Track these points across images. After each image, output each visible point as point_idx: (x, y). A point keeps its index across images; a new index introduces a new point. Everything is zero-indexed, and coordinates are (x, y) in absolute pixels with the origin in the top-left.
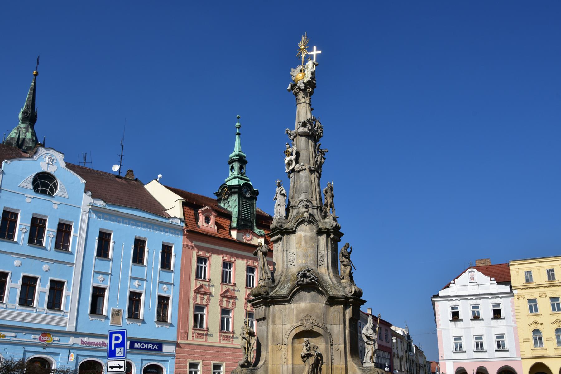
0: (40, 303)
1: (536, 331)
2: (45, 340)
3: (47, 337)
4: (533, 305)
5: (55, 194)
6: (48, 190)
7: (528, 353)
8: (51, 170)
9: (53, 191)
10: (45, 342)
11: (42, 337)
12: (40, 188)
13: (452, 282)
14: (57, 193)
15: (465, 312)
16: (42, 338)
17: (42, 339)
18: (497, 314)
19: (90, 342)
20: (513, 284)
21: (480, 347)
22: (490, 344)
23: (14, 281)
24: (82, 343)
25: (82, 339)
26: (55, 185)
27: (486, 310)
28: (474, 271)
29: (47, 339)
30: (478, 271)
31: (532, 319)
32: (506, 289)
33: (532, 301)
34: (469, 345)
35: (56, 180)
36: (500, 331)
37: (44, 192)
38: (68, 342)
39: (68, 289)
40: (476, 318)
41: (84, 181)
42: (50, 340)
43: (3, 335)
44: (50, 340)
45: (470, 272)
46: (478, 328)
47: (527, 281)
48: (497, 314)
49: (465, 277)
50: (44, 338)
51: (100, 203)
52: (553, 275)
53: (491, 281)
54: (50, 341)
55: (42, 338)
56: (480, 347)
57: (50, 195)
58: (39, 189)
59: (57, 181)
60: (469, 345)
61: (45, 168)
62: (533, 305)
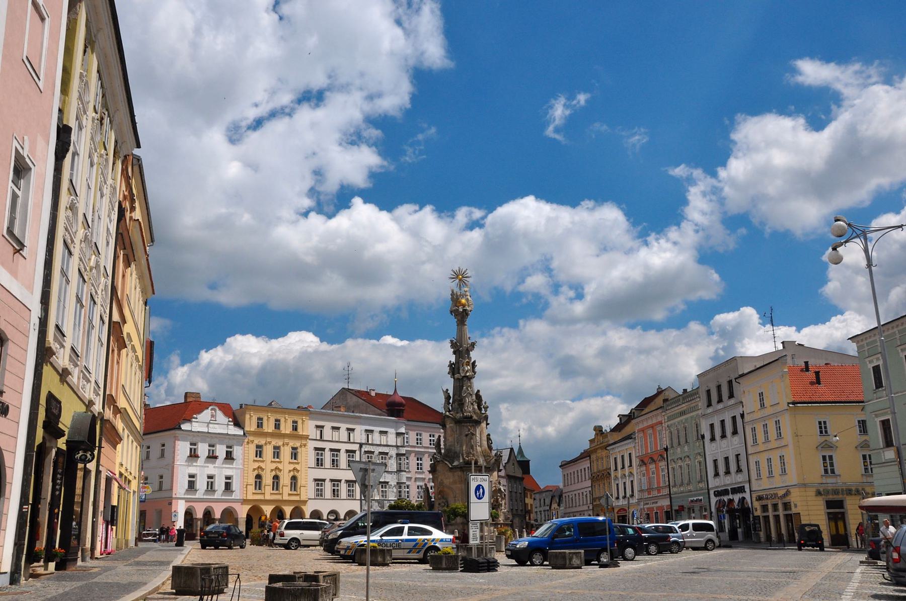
1: (258, 477)
4: (259, 451)
7: (250, 497)
13: (195, 416)
15: (203, 449)
18: (229, 456)
20: (247, 429)
21: (211, 487)
22: (220, 485)
27: (221, 451)
28: (214, 410)
30: (220, 409)
31: (256, 465)
32: (241, 433)
33: (259, 447)
34: (201, 484)
36: (229, 473)
40: (212, 457)
45: (212, 410)
46: (211, 469)
47: (258, 427)
48: (229, 456)
49: (206, 415)
52: (279, 425)
53: (229, 421)
56: (211, 487)
60: (201, 484)
62: (259, 451)
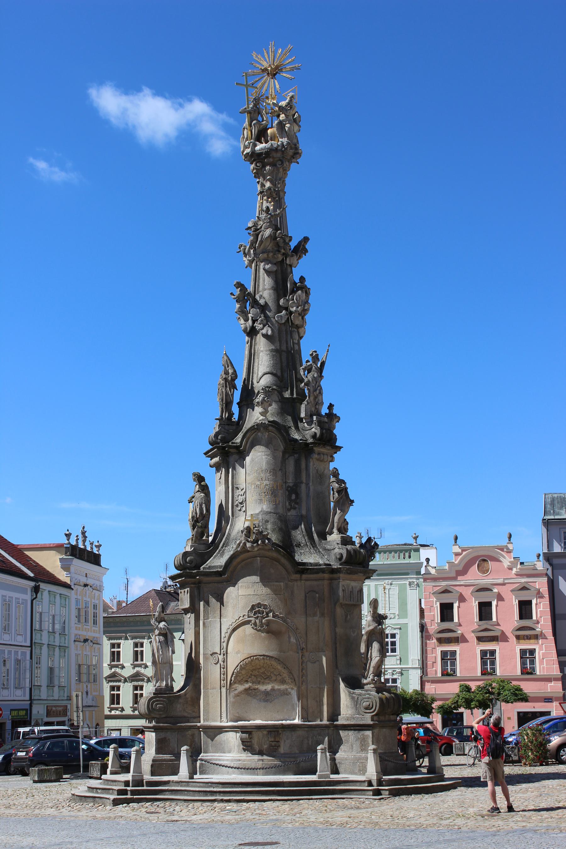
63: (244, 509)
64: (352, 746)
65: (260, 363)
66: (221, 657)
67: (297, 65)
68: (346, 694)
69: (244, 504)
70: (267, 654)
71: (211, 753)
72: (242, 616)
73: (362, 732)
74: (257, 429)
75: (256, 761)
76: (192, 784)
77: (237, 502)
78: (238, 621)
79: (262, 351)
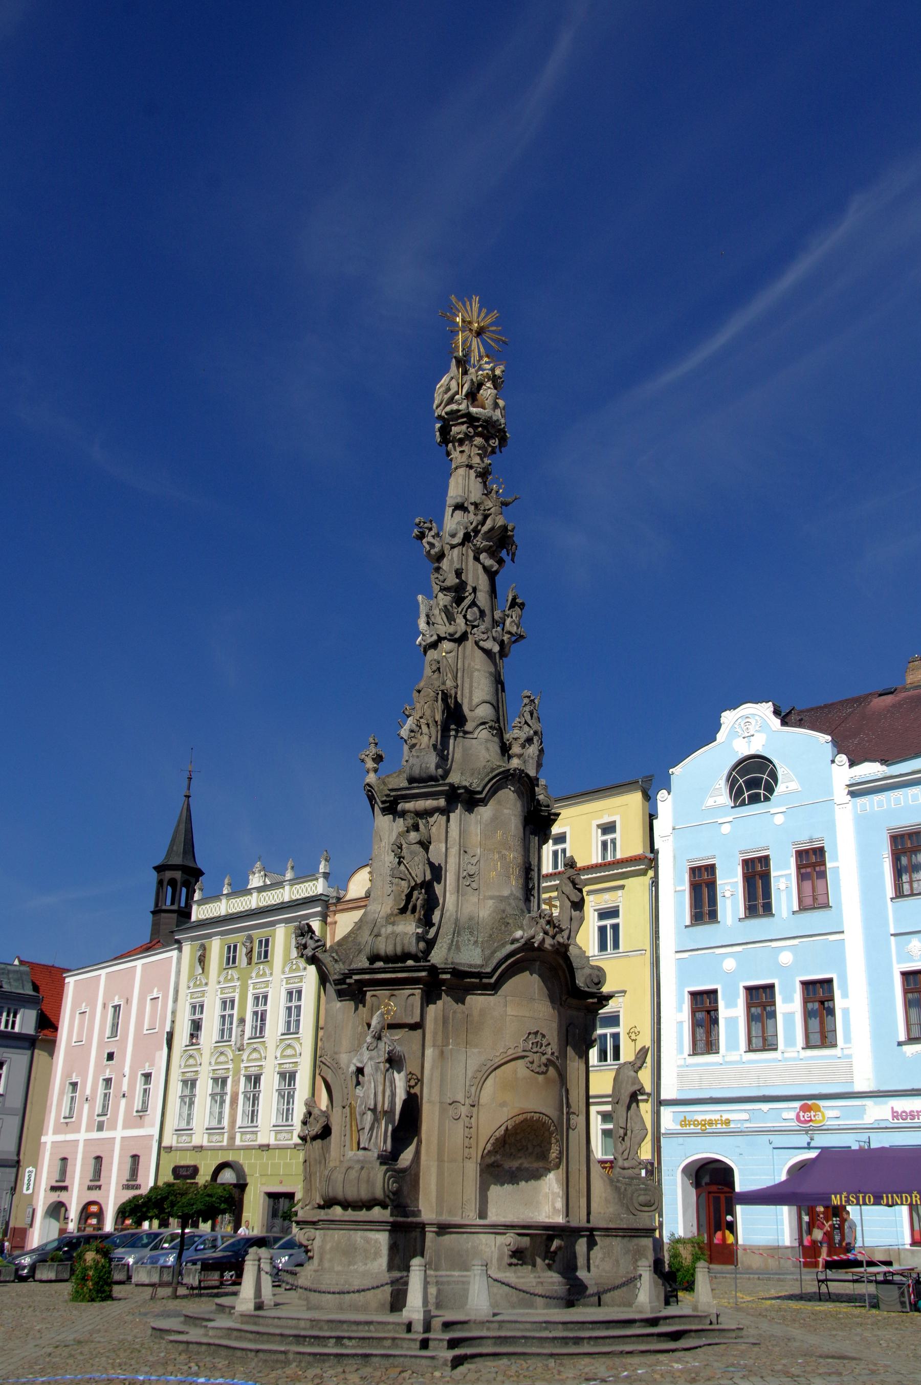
0: (790, 1042)
2: (811, 1121)
3: (812, 1113)
5: (775, 794)
6: (762, 791)
8: (755, 747)
9: (770, 789)
10: (811, 1124)
11: (801, 1114)
12: (746, 795)
14: (780, 789)
16: (804, 1117)
17: (802, 1119)
19: (913, 1111)
23: (788, 999)
24: (895, 1115)
25: (892, 1108)
26: (774, 775)
29: (813, 1118)
35: (771, 762)
37: (755, 799)
38: (862, 1118)
39: (845, 995)
41: (829, 738)
42: (821, 1118)
43: (727, 1120)
44: (821, 1118)
50: (806, 1116)
51: (870, 770)
54: (820, 1121)
55: (804, 1117)
57: (767, 799)
58: (744, 799)
59: (774, 766)
61: (744, 749)
63: (474, 885)
64: (617, 1261)
65: (475, 684)
66: (464, 1110)
67: (503, 338)
68: (604, 1181)
69: (476, 879)
70: (544, 1111)
71: (443, 1270)
72: (513, 1047)
73: (636, 1240)
74: (512, 775)
75: (534, 1285)
76: (508, 1325)
77: (465, 873)
78: (505, 1055)
79: (478, 670)
